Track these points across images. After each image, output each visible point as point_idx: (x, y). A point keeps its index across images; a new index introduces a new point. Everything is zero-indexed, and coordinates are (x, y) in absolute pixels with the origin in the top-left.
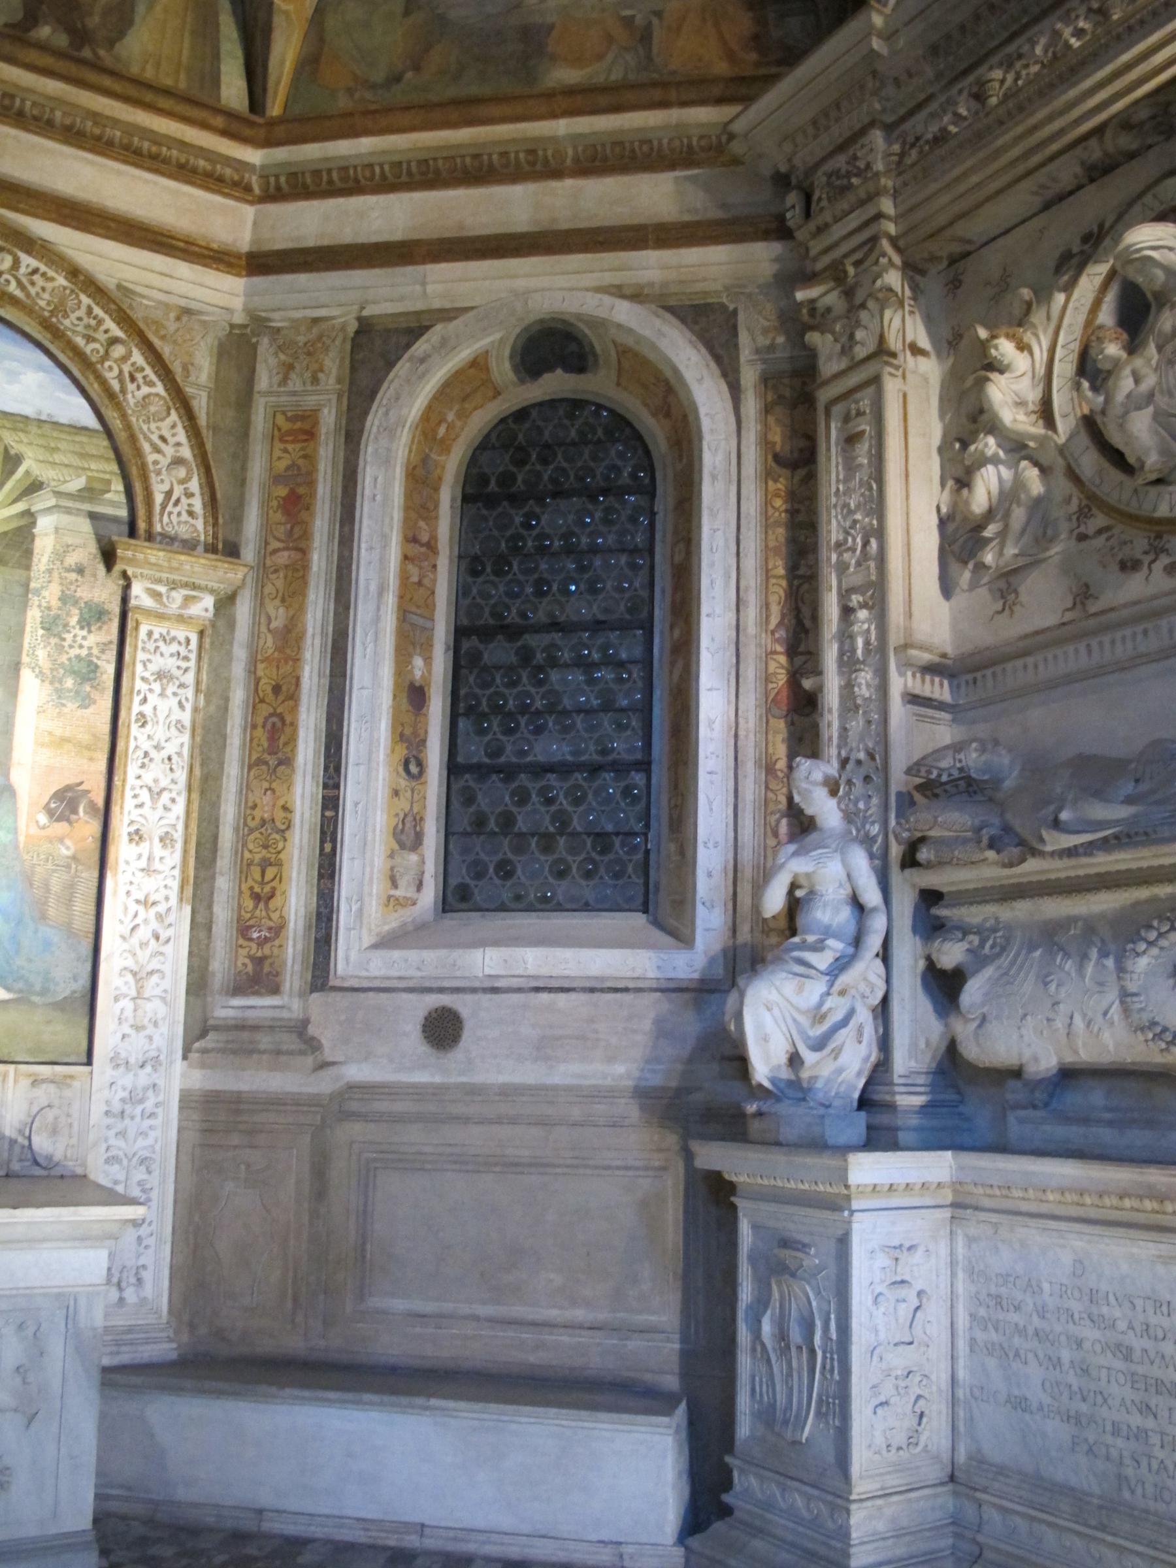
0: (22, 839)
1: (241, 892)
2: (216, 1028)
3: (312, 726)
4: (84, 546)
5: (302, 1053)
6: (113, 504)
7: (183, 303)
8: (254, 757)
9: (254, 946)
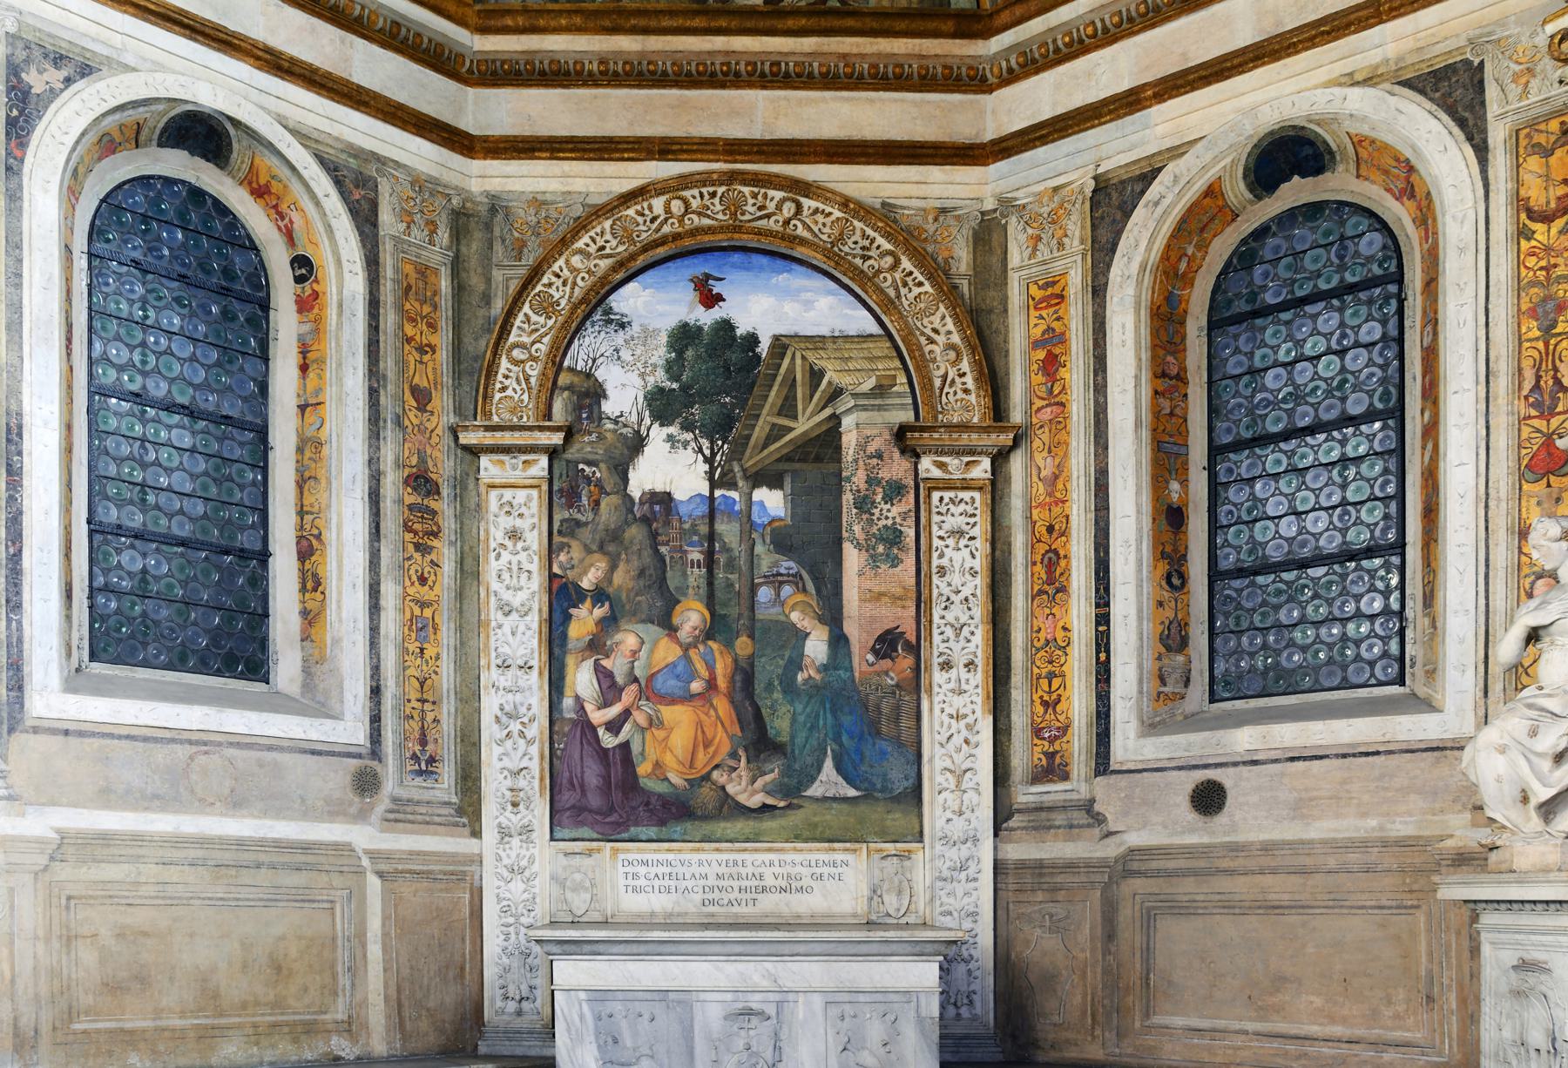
0: (857, 675)
1: (1032, 701)
2: (1019, 811)
3: (1083, 556)
4: (880, 435)
5: (1089, 826)
6: (899, 395)
7: (938, 204)
8: (1036, 588)
9: (1046, 743)
